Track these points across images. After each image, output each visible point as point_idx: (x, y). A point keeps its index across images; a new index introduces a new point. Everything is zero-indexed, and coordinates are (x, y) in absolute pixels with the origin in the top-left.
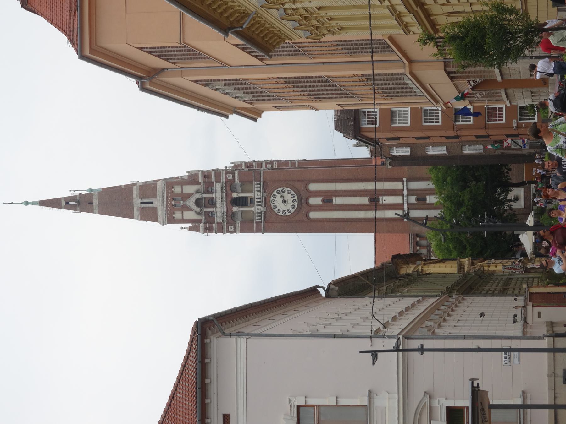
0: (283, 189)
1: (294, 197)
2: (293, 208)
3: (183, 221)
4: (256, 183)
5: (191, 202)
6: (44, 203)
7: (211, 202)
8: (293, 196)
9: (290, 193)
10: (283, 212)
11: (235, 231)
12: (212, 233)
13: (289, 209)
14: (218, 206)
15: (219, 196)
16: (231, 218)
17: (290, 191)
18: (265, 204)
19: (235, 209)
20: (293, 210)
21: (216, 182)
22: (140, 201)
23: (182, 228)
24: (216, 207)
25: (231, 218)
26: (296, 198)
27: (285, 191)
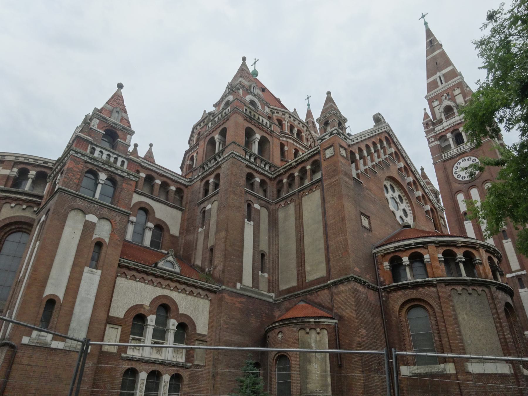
2: (462, 178)
3: (432, 109)
5: (447, 103)
6: (429, 33)
10: (456, 172)
11: (429, 143)
12: (425, 129)
13: (460, 175)
14: (448, 122)
16: (442, 137)
19: (449, 135)
20: (460, 179)
22: (441, 75)
23: (425, 109)
24: (447, 121)
25: (442, 137)
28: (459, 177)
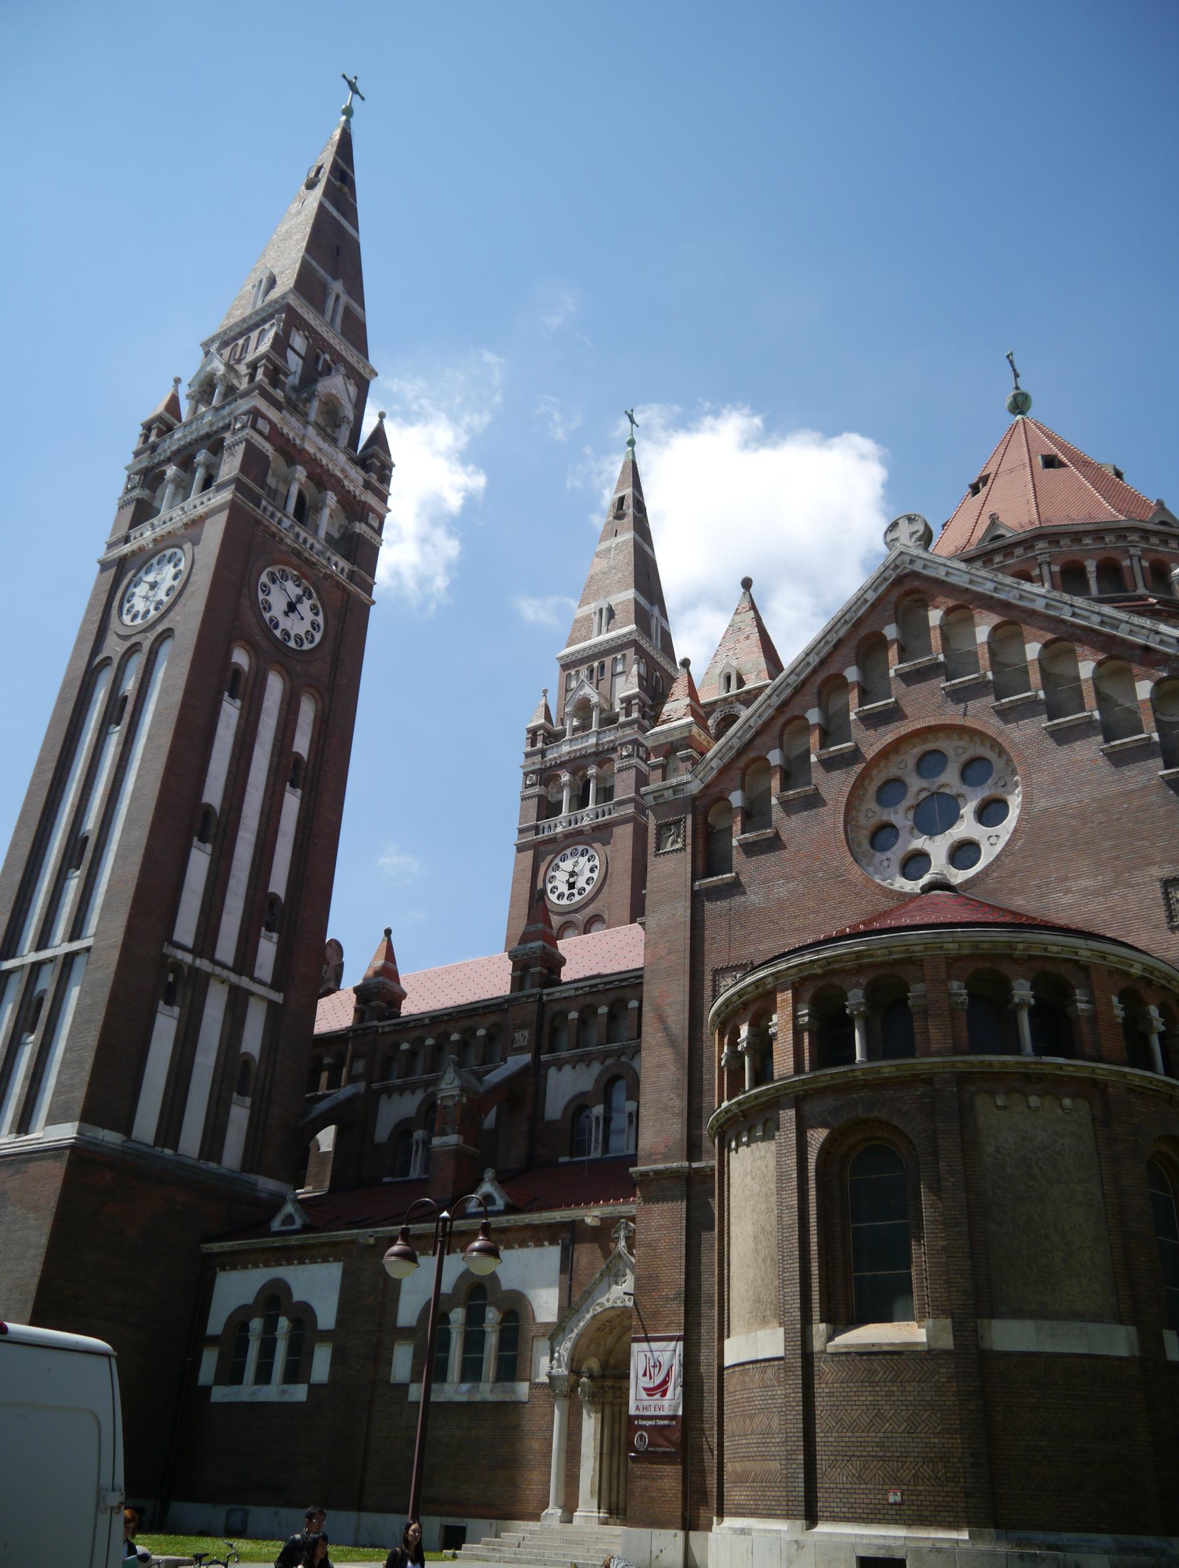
0: (318, 626)
1: (296, 642)
2: (271, 620)
4: (346, 570)
7: (328, 434)
8: (299, 640)
9: (307, 638)
10: (265, 586)
13: (270, 608)
15: (337, 461)
17: (311, 642)
18: (298, 554)
20: (267, 616)
21: (364, 480)
26: (292, 644)
27: (314, 629)
28: (265, 609)
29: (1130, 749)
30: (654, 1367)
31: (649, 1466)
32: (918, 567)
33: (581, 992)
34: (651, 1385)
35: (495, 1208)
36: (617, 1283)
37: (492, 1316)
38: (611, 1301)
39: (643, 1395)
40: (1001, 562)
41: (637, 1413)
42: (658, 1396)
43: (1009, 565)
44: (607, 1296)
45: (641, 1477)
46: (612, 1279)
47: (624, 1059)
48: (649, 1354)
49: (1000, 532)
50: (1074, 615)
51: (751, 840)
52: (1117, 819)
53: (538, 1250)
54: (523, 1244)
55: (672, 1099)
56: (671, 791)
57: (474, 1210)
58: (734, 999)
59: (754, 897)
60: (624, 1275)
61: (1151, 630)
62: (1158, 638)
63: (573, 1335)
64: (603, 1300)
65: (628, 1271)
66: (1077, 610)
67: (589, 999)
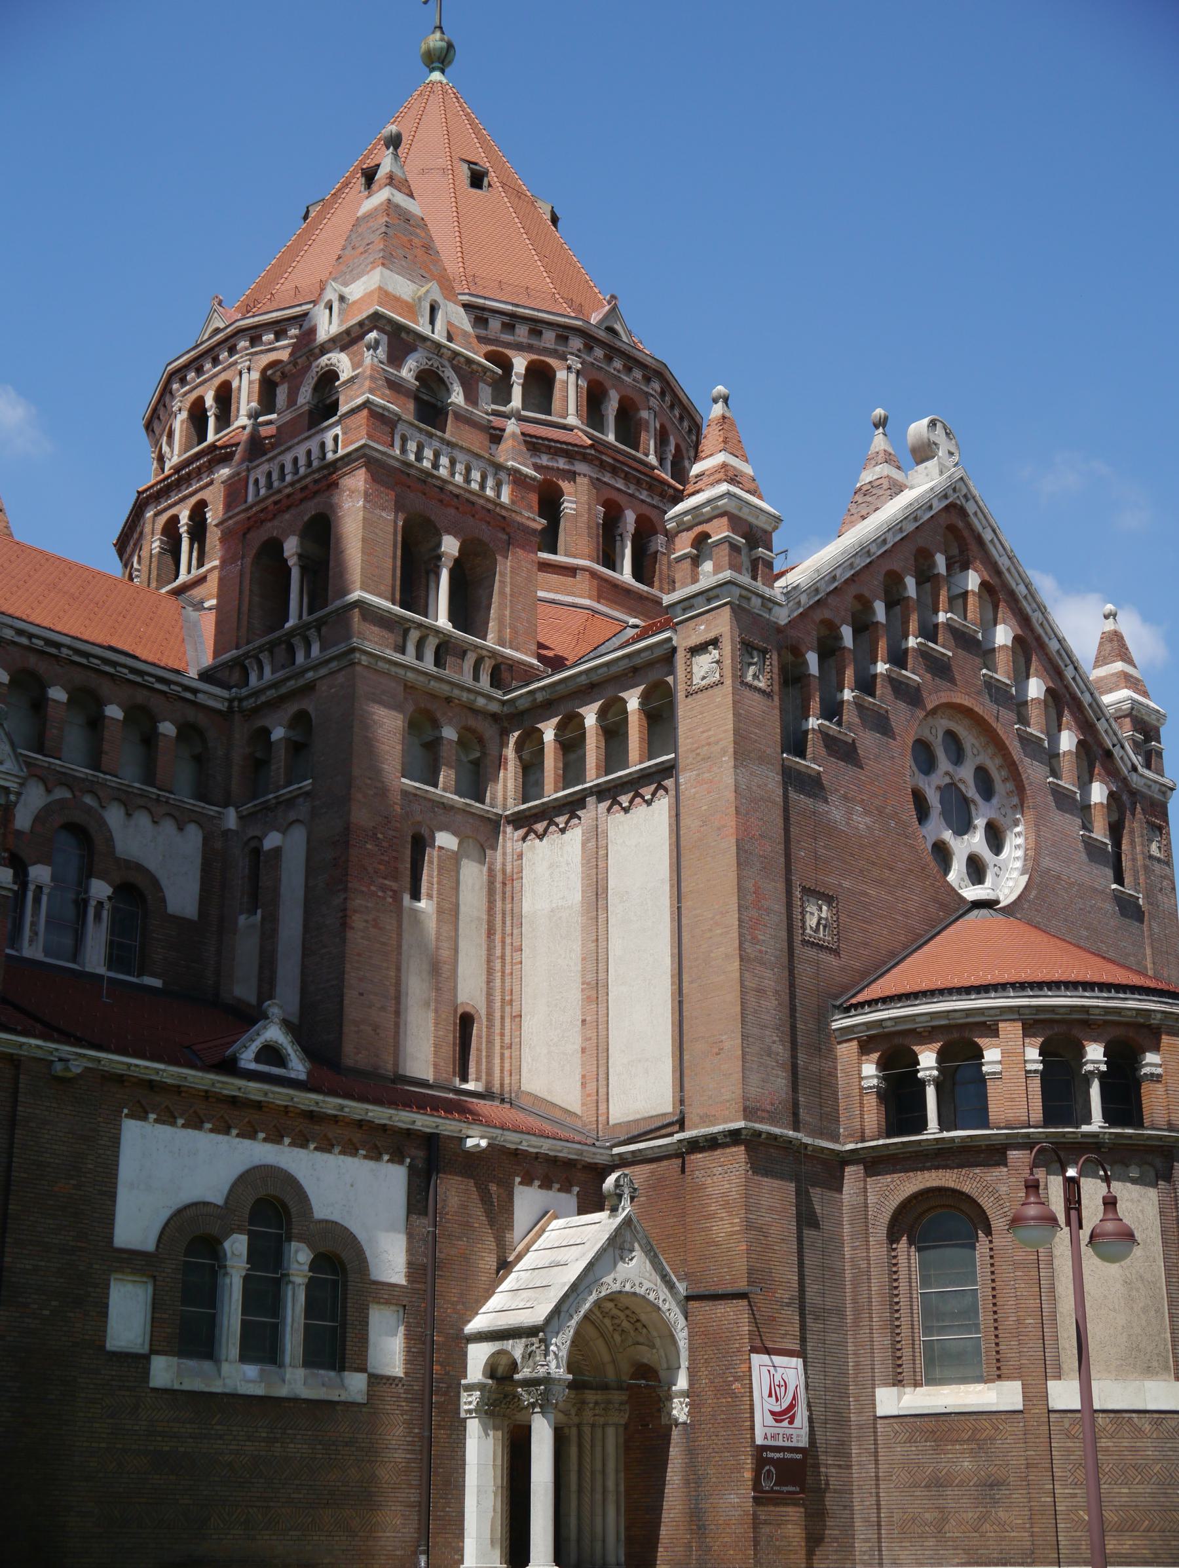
29: (1096, 847)
30: (779, 1386)
31: (772, 1508)
32: (970, 508)
33: (24, 641)
34: (777, 1409)
35: (293, 1075)
36: (622, 1259)
37: (300, 1257)
38: (618, 1282)
39: (770, 1420)
40: (619, 371)
41: (766, 1443)
42: (785, 1423)
43: (622, 381)
44: (612, 1276)
45: (766, 1522)
46: (618, 1252)
47: (88, 800)
48: (772, 1369)
49: (618, 327)
50: (1074, 679)
51: (831, 733)
52: (1090, 912)
53: (371, 1164)
54: (350, 1149)
55: (774, 1042)
56: (759, 601)
57: (253, 1066)
58: (1097, 1011)
59: (835, 812)
60: (632, 1251)
61: (1120, 742)
62: (1122, 753)
63: (573, 1323)
64: (608, 1279)
65: (636, 1245)
66: (1078, 677)
67: (32, 661)
